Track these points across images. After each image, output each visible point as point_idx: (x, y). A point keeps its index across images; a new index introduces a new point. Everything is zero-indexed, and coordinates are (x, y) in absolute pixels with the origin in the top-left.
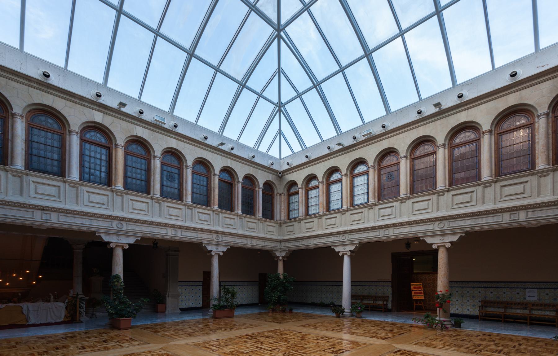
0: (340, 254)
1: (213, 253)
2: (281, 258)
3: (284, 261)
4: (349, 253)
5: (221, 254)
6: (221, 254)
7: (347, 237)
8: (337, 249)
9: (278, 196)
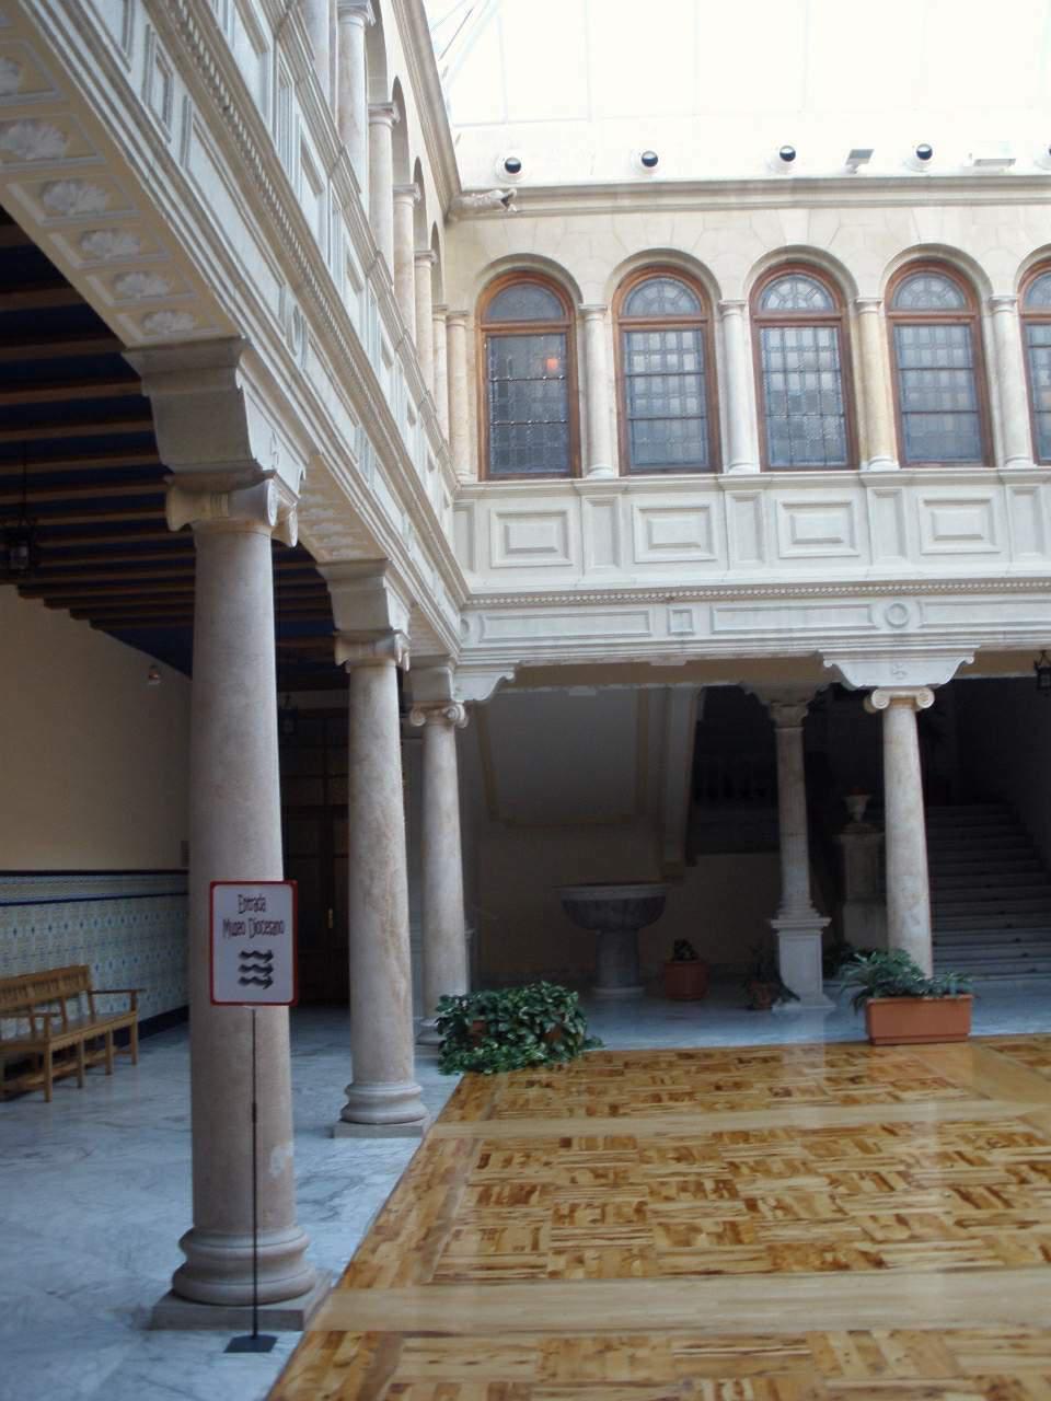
7: (919, 617)
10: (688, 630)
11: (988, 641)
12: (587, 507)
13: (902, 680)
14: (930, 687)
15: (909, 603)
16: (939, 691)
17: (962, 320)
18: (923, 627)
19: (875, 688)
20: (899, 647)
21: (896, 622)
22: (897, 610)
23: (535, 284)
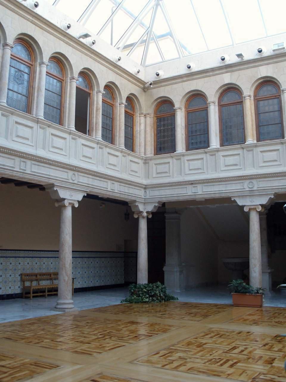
1: (66, 203)
2: (145, 214)
4: (260, 209)
5: (76, 205)
6: (76, 205)
7: (257, 185)
8: (240, 202)
9: (142, 119)
10: (197, 192)
11: (277, 191)
12: (175, 160)
14: (260, 205)
15: (254, 181)
17: (277, 97)
18: (258, 188)
19: (245, 206)
20: (251, 194)
21: (250, 187)
22: (251, 183)
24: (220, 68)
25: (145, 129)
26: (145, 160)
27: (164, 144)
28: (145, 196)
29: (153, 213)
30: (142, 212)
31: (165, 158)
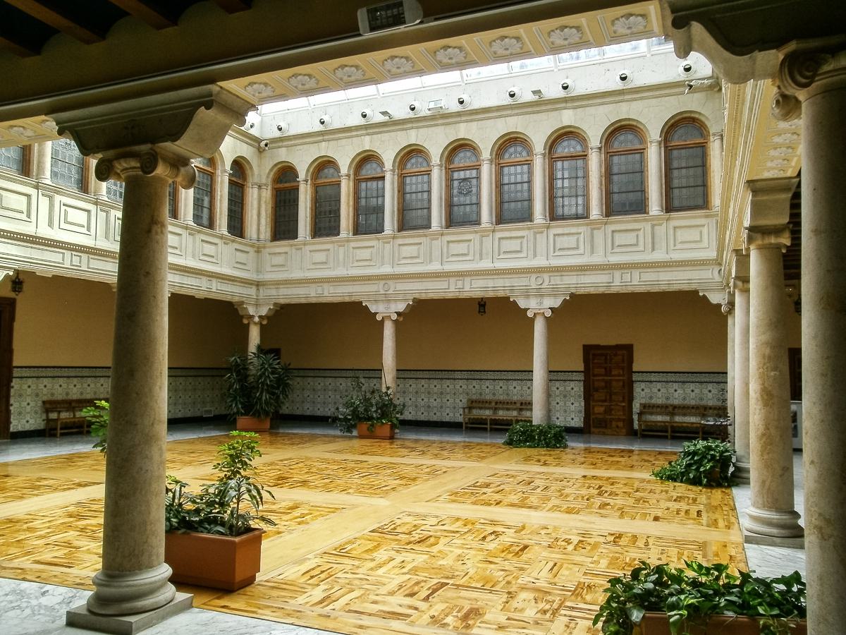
0: (379, 318)
2: (257, 319)
3: (261, 324)
4: (394, 317)
9: (256, 191)
11: (417, 296)
12: (294, 251)
13: (387, 309)
15: (391, 283)
16: (399, 314)
23: (285, 174)
24: (358, 128)
25: (258, 206)
26: (258, 248)
27: (284, 227)
28: (257, 296)
29: (267, 317)
30: (253, 316)
31: (283, 246)
